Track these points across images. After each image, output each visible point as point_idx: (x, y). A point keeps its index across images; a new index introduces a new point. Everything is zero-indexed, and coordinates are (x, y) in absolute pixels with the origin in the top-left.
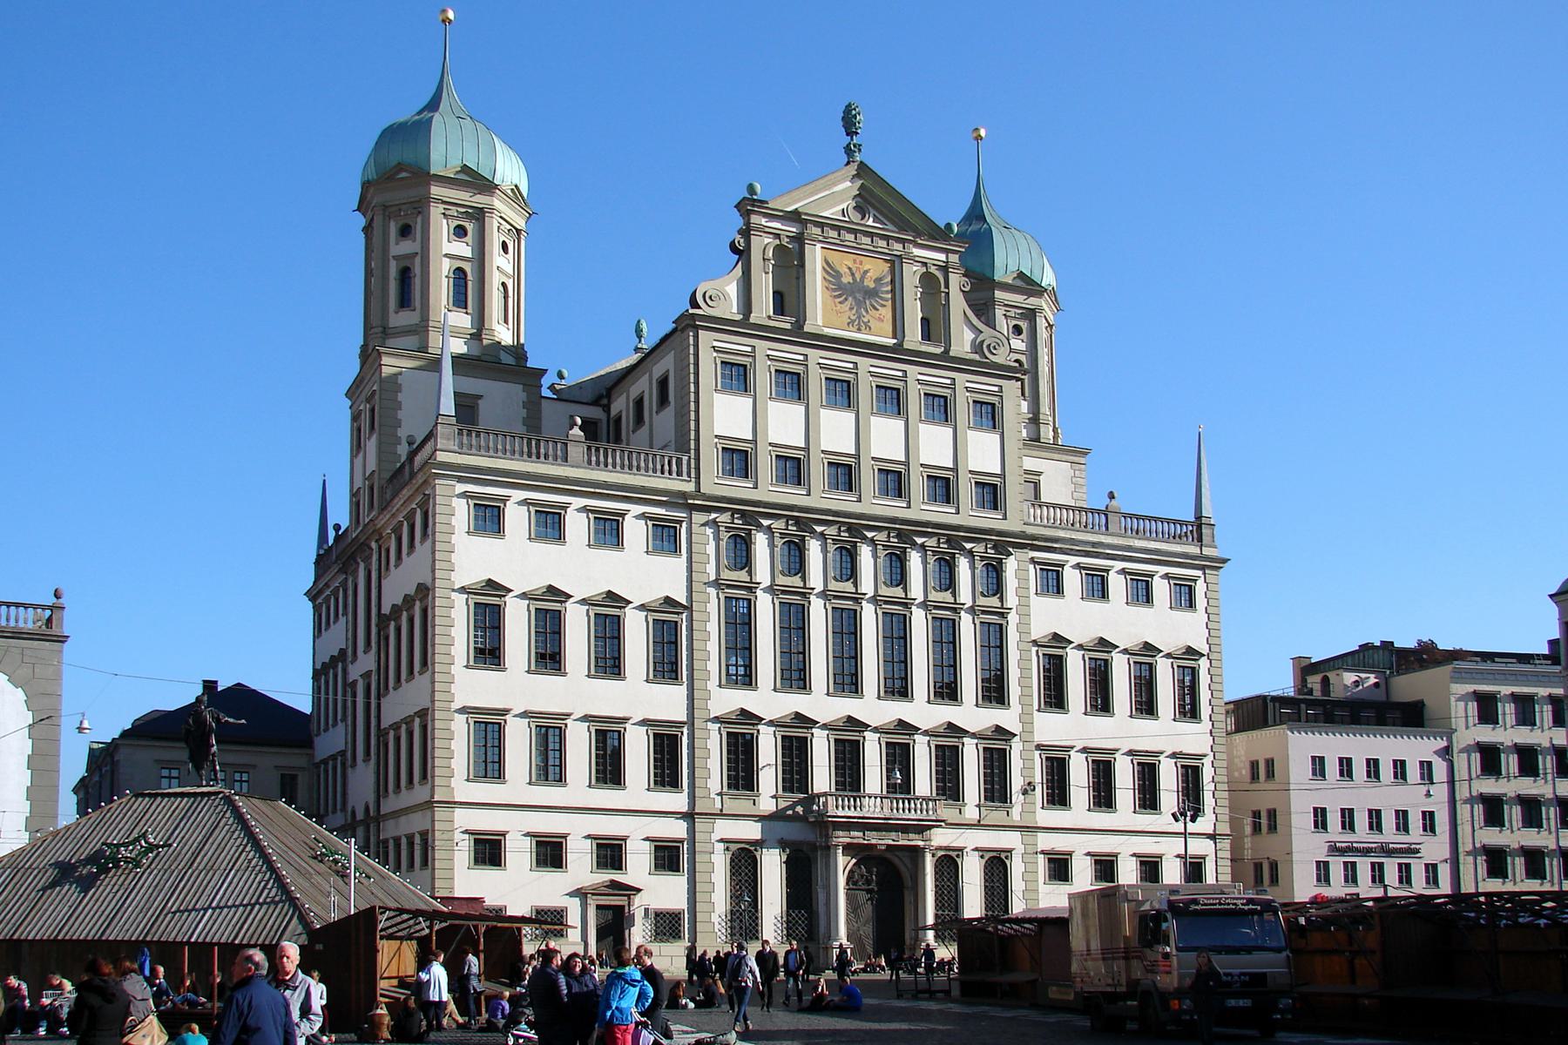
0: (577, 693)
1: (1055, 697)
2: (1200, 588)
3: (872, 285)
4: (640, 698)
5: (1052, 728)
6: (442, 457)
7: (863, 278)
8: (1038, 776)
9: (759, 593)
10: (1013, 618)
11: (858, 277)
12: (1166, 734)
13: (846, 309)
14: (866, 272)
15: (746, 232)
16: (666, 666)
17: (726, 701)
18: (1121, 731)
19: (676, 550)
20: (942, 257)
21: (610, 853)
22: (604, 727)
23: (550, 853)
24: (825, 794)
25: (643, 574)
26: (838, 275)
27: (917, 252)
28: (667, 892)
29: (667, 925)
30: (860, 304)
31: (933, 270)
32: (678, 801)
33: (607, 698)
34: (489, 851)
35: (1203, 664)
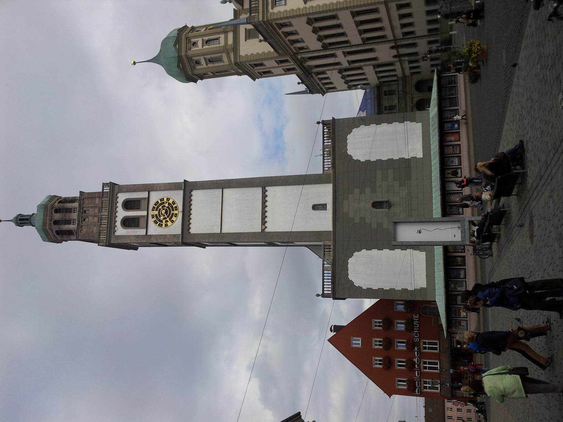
6: (261, 19)
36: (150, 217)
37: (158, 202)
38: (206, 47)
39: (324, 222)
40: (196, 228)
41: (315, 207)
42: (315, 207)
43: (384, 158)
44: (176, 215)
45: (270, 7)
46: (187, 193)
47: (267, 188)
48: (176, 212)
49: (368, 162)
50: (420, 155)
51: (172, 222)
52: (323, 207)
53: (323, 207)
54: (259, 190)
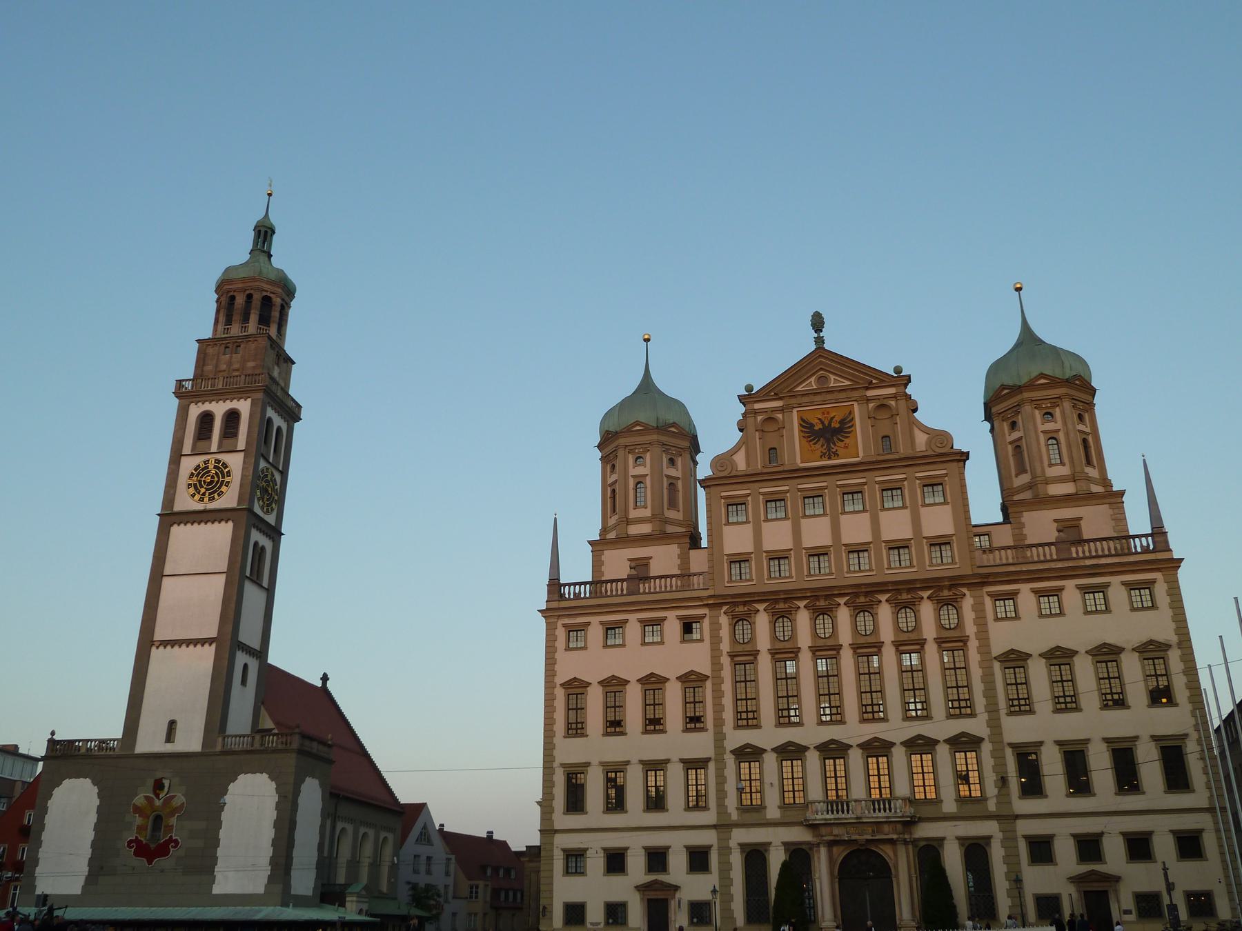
0: (635, 745)
2: (1161, 589)
3: (837, 426)
4: (677, 743)
7: (830, 423)
10: (973, 644)
11: (826, 423)
12: (1142, 722)
13: (819, 447)
15: (744, 415)
16: (694, 722)
17: (737, 738)
18: (1094, 725)
20: (892, 391)
21: (657, 859)
23: (616, 862)
24: (814, 802)
25: (675, 656)
26: (812, 425)
27: (870, 393)
28: (696, 887)
30: (828, 441)
31: (885, 402)
33: (654, 746)
34: (575, 860)
35: (1174, 656)
36: (205, 458)
37: (192, 474)
38: (631, 483)
39: (150, 741)
40: (179, 533)
41: (172, 724)
42: (172, 724)
43: (222, 834)
44: (201, 500)
45: (567, 621)
46: (229, 514)
47: (214, 645)
48: (206, 500)
49: (221, 807)
50: (216, 890)
51: (193, 496)
52: (170, 738)
53: (170, 738)
54: (214, 634)
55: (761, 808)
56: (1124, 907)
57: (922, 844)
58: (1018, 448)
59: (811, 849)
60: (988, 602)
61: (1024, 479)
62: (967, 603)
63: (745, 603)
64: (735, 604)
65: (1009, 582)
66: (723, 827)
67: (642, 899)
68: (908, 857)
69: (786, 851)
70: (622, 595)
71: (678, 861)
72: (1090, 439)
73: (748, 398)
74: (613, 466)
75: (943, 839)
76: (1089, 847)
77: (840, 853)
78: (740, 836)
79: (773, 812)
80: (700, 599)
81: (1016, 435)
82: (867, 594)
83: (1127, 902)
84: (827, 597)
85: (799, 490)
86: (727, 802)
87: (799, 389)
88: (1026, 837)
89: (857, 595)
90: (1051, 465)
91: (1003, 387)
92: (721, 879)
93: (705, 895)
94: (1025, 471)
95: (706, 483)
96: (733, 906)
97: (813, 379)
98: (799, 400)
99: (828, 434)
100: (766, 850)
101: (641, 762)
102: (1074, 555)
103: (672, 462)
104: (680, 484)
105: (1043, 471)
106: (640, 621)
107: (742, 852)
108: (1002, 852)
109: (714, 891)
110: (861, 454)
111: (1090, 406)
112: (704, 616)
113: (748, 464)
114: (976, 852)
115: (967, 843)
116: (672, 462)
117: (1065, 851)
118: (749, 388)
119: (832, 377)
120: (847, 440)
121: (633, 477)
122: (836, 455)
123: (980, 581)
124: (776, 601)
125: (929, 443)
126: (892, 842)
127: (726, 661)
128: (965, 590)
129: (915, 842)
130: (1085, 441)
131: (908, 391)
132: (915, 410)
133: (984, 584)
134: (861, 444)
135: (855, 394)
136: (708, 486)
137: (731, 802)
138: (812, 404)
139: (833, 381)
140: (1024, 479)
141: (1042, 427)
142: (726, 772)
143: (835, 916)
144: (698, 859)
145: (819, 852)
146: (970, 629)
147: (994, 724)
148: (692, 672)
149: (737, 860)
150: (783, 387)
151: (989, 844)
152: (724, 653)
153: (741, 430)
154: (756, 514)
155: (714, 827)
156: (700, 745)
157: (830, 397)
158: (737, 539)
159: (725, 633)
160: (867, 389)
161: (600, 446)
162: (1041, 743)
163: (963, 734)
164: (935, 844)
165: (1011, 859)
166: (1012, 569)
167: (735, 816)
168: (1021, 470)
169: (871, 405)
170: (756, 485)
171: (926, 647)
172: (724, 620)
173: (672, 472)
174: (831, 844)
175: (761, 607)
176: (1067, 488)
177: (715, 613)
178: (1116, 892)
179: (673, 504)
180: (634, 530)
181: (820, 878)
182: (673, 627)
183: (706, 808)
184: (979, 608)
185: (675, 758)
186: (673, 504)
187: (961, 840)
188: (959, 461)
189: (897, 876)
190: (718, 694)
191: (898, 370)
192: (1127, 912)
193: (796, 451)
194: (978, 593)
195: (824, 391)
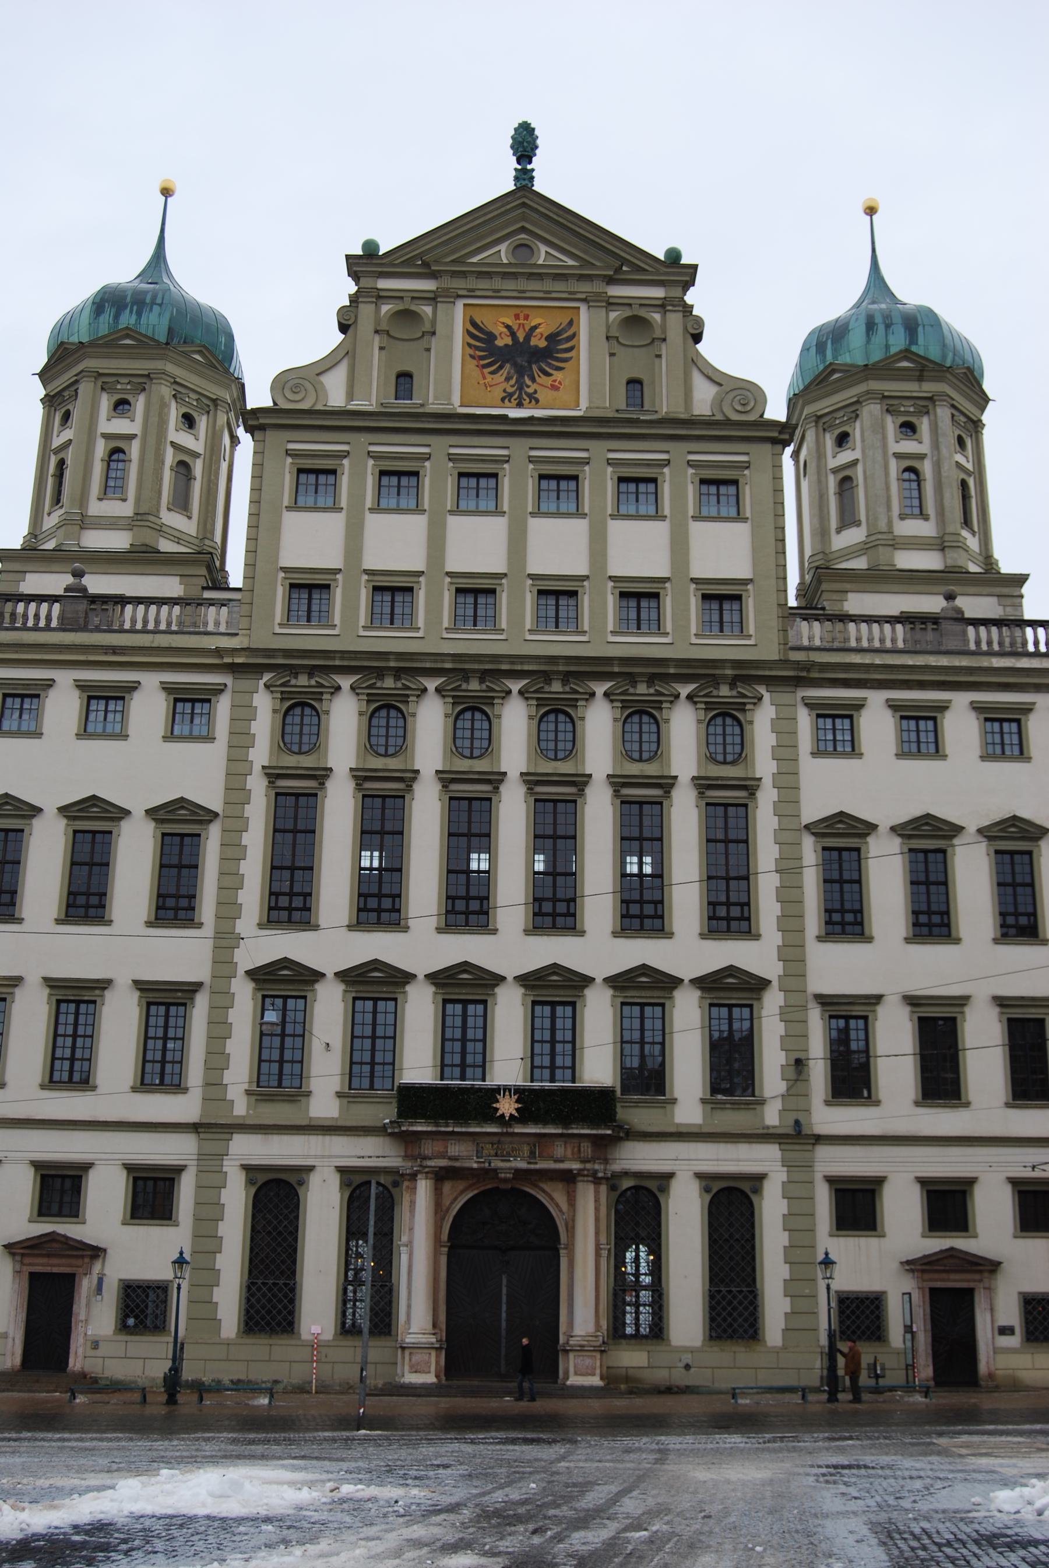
1: (846, 919)
3: (543, 344)
4: (129, 949)
5: (838, 968)
7: (528, 336)
8: (817, 1047)
9: (330, 785)
10: (767, 798)
11: (521, 335)
13: (500, 381)
14: (535, 327)
15: (354, 299)
16: (174, 905)
19: (209, 738)
20: (658, 293)
22: (70, 995)
25: (148, 765)
26: (491, 337)
28: (142, 1253)
29: (143, 1307)
31: (643, 313)
32: (184, 1107)
38: (101, 449)
55: (300, 1094)
56: (1003, 1321)
57: (627, 1183)
58: (846, 483)
59: (396, 1184)
60: (804, 720)
61: (855, 536)
62: (762, 721)
63: (312, 671)
64: (294, 671)
65: (847, 684)
66: (212, 1129)
67: (17, 1273)
68: (597, 1209)
69: (344, 1184)
70: (48, 628)
71: (106, 1196)
72: (971, 482)
73: (365, 264)
74: (67, 417)
75: (670, 1176)
76: (947, 1204)
77: (458, 1197)
78: (249, 1149)
79: (324, 1100)
80: (218, 652)
81: (846, 457)
82: (566, 677)
83: (1010, 1312)
84: (483, 675)
85: (452, 458)
86: (228, 1077)
87: (475, 260)
88: (831, 1180)
89: (547, 677)
90: (902, 517)
91: (831, 369)
92: (196, 1236)
93: (159, 1270)
94: (858, 523)
95: (257, 422)
96: (218, 1294)
97: (503, 248)
98: (472, 283)
99: (523, 359)
100: (301, 1183)
101: (51, 983)
102: (972, 646)
103: (189, 421)
104: (198, 468)
105: (890, 524)
106: (81, 686)
107: (250, 1182)
108: (783, 1206)
109: (180, 1262)
110: (584, 404)
111: (976, 426)
112: (219, 690)
113: (350, 396)
114: (731, 1207)
115: (716, 1187)
116: (189, 421)
117: (902, 1210)
118: (370, 248)
119: (543, 249)
120: (558, 376)
121: (106, 436)
122: (534, 399)
123: (792, 675)
124: (380, 673)
125: (718, 402)
126: (568, 1178)
127: (257, 785)
128: (762, 690)
129: (612, 1181)
130: (964, 484)
131: (690, 298)
132: (697, 338)
133: (798, 682)
134: (586, 384)
135: (585, 287)
136: (262, 428)
137: (239, 1074)
138: (497, 294)
139: (542, 254)
140: (855, 536)
141: (895, 447)
142: (233, 1016)
143: (435, 1325)
144: (151, 1195)
145: (414, 1189)
146: (764, 765)
147: (793, 956)
148: (181, 803)
149: (236, 1200)
150: (442, 256)
151: (758, 1191)
152: (257, 768)
153: (343, 328)
154: (357, 497)
155: (195, 1128)
156: (181, 956)
157: (535, 285)
158: (312, 540)
159: (263, 725)
160: (610, 281)
161: (45, 375)
162: (878, 999)
163: (731, 970)
164: (652, 1185)
165: (798, 1223)
166: (856, 659)
167: (241, 1108)
168: (848, 519)
169: (613, 315)
170: (363, 438)
171: (676, 794)
172: (264, 705)
173: (185, 439)
174: (441, 1176)
175: (345, 682)
176: (928, 561)
177: (245, 684)
178: (989, 1289)
179: (181, 503)
180: (95, 540)
181: (410, 1244)
182: (149, 707)
183: (178, 1087)
184: (785, 729)
185: (123, 980)
186: (181, 503)
187: (704, 1178)
188: (774, 441)
189: (570, 1247)
190: (233, 852)
191: (674, 256)
192: (1006, 1331)
193: (452, 379)
194: (785, 698)
195: (523, 272)
